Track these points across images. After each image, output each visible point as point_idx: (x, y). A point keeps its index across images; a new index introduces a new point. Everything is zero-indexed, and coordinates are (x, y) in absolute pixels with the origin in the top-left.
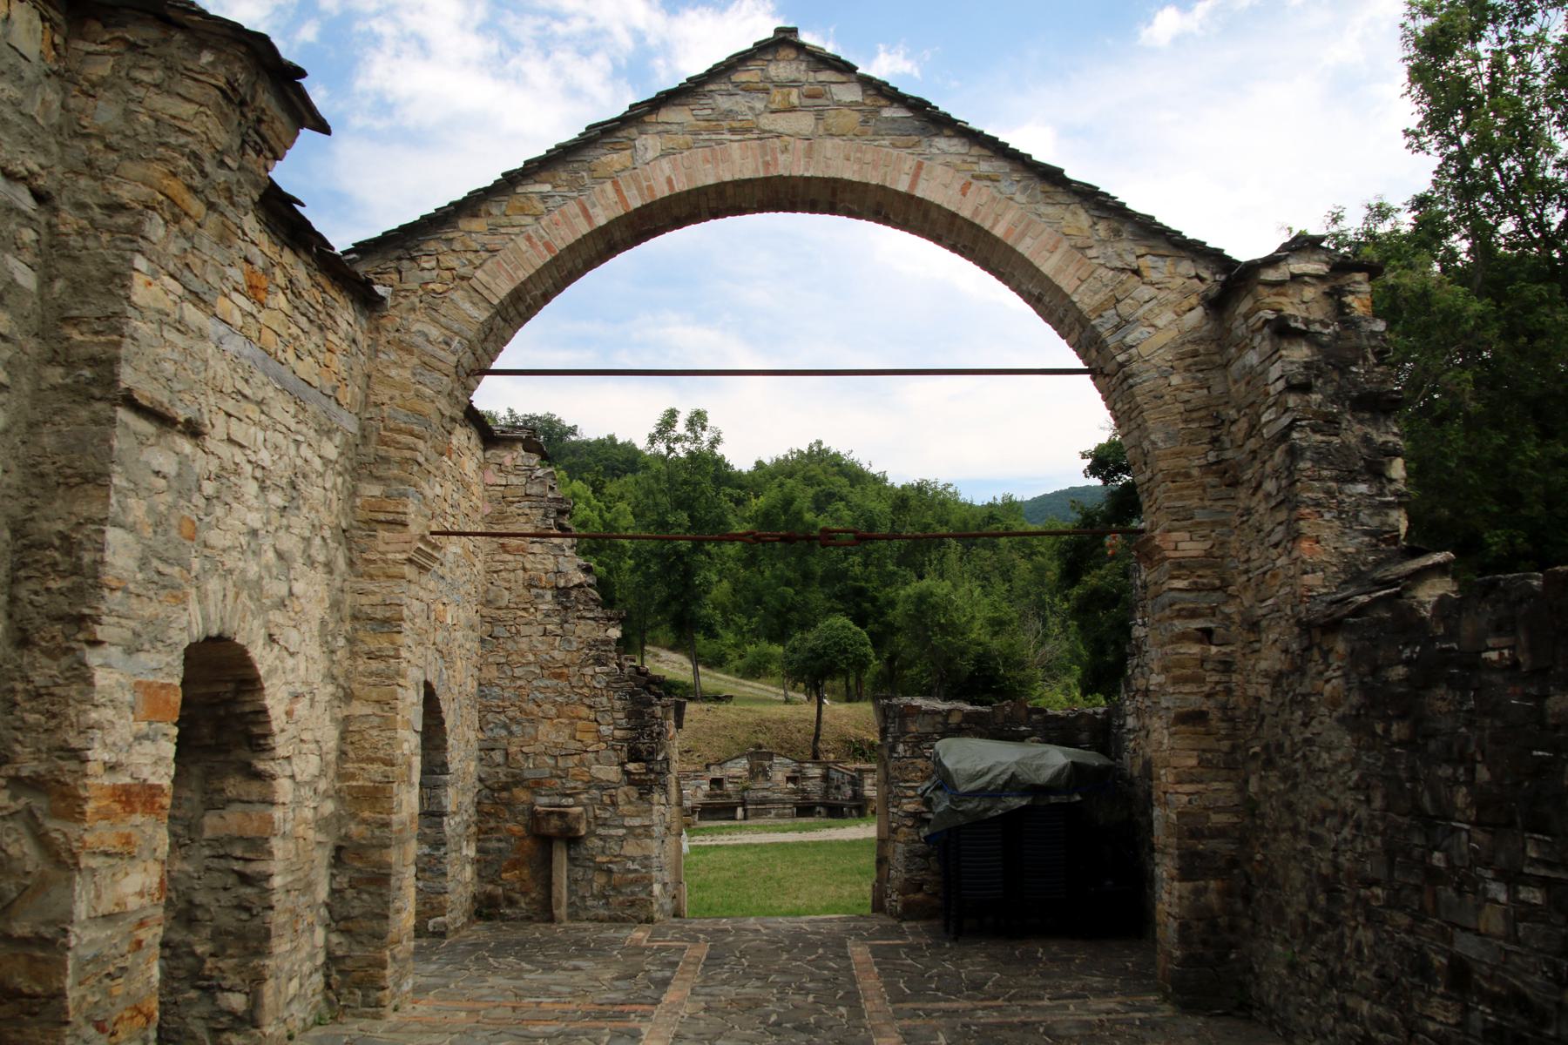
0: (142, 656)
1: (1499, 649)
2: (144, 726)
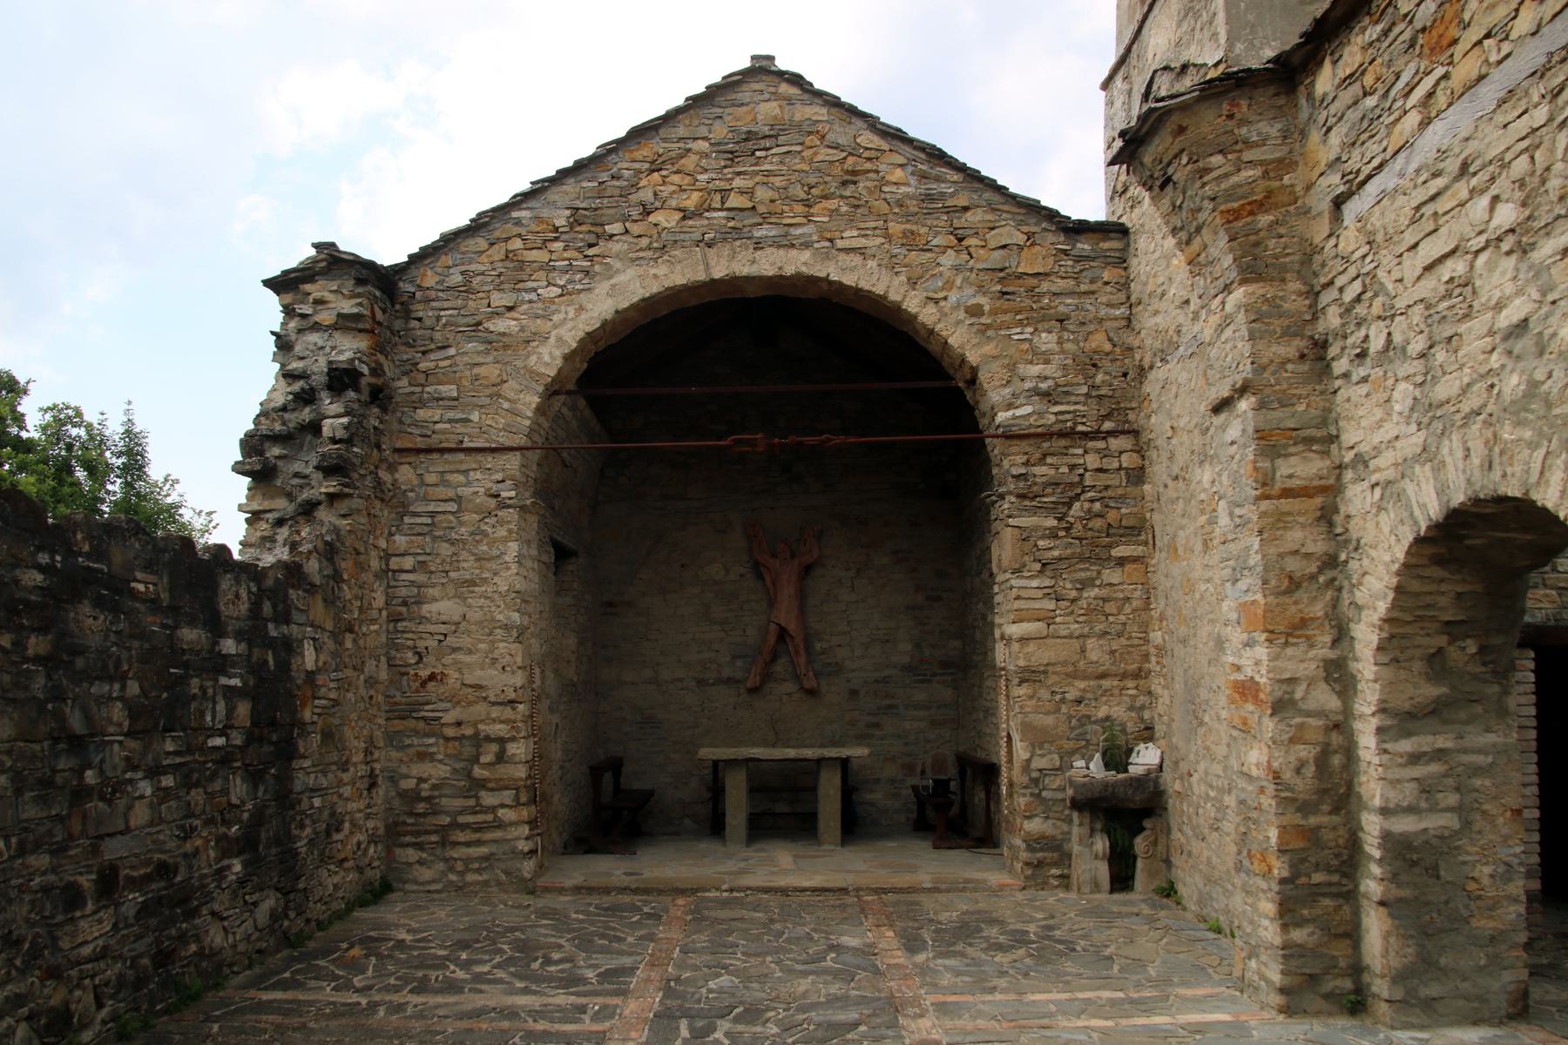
1: (146, 583)
2: (1245, 635)
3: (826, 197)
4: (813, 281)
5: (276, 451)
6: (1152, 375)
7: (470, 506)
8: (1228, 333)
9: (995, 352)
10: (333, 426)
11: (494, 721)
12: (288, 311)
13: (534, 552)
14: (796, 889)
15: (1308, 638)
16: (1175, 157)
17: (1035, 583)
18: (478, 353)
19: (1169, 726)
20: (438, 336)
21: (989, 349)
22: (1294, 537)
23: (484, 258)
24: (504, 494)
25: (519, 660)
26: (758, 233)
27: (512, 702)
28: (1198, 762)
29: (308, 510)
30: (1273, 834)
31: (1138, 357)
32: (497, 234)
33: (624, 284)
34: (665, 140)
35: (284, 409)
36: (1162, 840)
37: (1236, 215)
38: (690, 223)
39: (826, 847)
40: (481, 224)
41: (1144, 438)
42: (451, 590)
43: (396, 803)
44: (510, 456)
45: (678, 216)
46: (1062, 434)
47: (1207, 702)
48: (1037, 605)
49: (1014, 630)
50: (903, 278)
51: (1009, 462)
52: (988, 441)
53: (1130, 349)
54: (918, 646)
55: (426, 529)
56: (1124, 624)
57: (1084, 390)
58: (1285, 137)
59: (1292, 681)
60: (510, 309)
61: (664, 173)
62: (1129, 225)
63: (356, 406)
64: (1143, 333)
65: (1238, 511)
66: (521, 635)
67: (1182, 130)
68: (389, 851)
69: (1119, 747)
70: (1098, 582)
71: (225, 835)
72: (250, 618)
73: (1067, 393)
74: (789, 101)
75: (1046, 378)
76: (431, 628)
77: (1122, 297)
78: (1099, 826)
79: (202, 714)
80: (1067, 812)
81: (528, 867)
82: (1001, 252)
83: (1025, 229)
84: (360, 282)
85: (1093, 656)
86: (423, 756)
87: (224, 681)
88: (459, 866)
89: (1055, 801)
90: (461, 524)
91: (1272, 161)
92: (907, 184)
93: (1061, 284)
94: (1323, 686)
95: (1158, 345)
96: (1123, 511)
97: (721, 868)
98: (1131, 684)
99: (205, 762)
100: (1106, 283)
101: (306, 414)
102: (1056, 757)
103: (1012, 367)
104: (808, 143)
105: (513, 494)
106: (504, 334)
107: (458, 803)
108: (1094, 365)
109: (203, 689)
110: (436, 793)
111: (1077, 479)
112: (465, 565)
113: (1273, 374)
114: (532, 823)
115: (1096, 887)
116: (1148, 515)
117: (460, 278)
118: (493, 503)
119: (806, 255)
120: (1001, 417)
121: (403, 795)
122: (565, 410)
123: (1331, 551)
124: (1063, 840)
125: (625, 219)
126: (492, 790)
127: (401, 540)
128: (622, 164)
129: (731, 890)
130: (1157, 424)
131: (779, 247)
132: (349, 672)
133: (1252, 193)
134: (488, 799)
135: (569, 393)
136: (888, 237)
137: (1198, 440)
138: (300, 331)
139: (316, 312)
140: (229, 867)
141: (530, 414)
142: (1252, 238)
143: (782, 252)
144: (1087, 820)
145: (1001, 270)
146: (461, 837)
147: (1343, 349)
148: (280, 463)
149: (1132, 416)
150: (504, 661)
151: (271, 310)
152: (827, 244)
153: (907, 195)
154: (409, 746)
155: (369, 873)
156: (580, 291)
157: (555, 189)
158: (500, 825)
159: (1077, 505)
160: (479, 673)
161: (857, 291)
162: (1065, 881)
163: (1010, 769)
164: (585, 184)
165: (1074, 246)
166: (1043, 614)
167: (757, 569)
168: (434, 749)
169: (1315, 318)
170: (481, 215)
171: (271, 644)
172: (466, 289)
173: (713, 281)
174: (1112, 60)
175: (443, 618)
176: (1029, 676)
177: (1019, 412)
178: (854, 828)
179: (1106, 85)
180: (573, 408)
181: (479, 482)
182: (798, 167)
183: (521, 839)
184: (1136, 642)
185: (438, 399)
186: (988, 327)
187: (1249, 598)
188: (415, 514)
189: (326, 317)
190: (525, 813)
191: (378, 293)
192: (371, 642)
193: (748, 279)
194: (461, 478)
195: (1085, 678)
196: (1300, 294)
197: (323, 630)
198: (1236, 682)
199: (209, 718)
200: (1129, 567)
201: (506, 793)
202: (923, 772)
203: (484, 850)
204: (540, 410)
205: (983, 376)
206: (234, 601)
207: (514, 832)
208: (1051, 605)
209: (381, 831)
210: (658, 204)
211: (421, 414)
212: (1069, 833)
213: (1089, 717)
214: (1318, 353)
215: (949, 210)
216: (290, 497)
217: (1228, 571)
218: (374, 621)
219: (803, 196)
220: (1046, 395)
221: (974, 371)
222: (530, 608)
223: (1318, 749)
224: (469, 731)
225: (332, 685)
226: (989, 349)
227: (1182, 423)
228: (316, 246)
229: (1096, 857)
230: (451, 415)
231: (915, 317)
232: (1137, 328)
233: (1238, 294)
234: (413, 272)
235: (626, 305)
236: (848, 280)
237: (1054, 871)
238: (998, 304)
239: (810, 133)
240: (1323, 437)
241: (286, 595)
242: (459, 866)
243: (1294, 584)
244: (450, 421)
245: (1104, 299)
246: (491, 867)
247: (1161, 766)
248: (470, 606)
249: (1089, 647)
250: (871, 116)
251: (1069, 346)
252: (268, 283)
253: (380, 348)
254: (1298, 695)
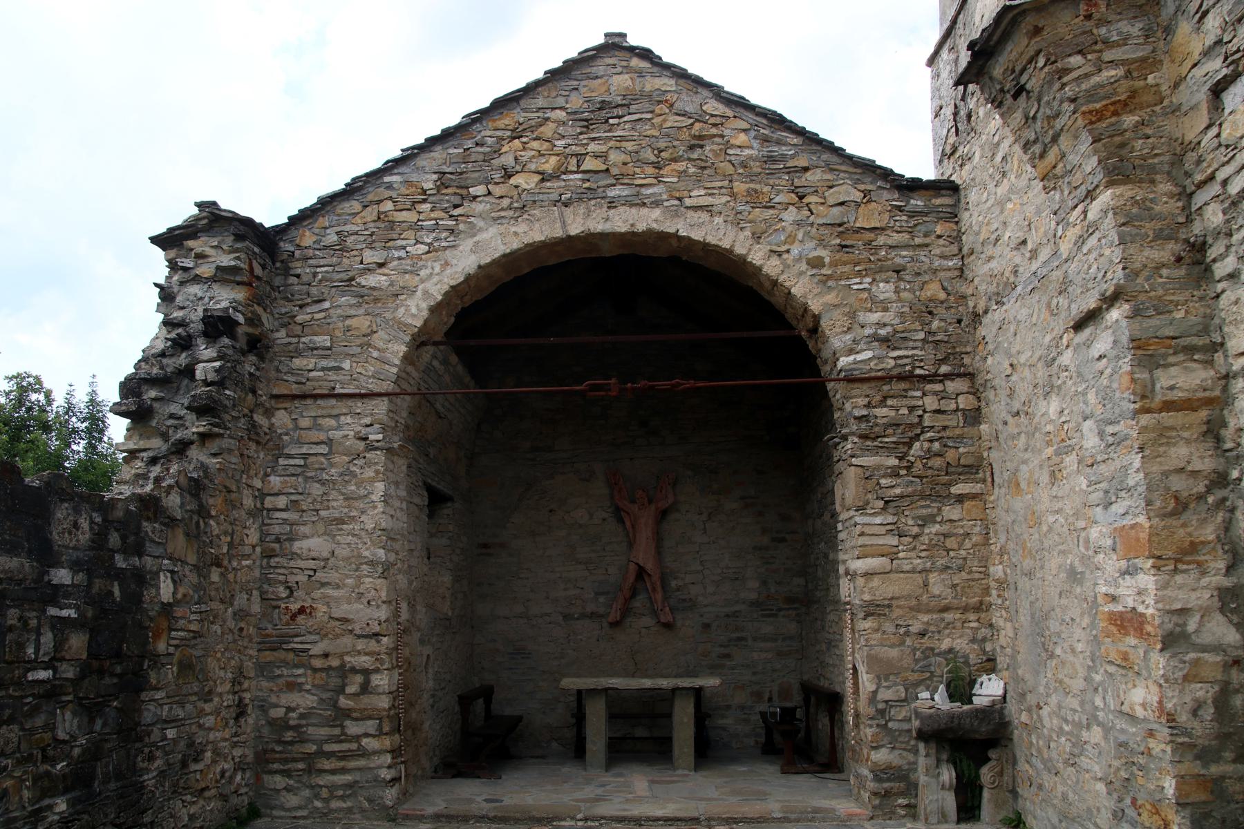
0: (1114, 507)
2: (1123, 563)
3: (675, 160)
4: (663, 237)
5: (153, 393)
6: (986, 320)
7: (340, 449)
8: (1092, 241)
9: (836, 302)
11: (359, 652)
12: (173, 265)
13: (404, 494)
14: (649, 819)
15: (1199, 564)
16: (1030, 62)
17: (878, 520)
18: (351, 306)
19: (1013, 657)
20: (314, 291)
21: (830, 298)
22: (1179, 453)
23: (358, 220)
24: (372, 437)
25: (384, 594)
26: (612, 193)
27: (376, 635)
28: (1048, 695)
29: (181, 449)
30: (1170, 786)
31: (971, 304)
32: (370, 197)
34: (525, 110)
35: (163, 354)
36: (1008, 771)
37: (1099, 115)
38: (548, 184)
39: (680, 772)
40: (353, 189)
41: (979, 380)
42: (321, 528)
43: (266, 731)
44: (378, 401)
45: (537, 178)
46: (901, 378)
47: (1059, 634)
48: (881, 541)
49: (859, 565)
50: (748, 233)
51: (851, 405)
52: (830, 386)
53: (964, 297)
54: (764, 583)
55: (299, 470)
56: (965, 559)
57: (921, 335)
58: (1147, 37)
59: (1183, 611)
60: (381, 265)
61: (524, 140)
62: (959, 182)
63: (230, 352)
64: (976, 281)
65: (1110, 429)
66: (386, 571)
67: (1037, 31)
68: (258, 778)
69: (963, 679)
70: (939, 519)
71: (48, 773)
72: (91, 548)
73: (905, 339)
74: (640, 73)
75: (885, 325)
76: (302, 564)
77: (954, 249)
78: (945, 756)
79: (21, 646)
80: (913, 742)
81: (390, 795)
82: (840, 208)
83: (862, 187)
84: (239, 237)
85: (936, 590)
86: (292, 686)
87: (53, 611)
88: (324, 793)
89: (901, 731)
90: (332, 465)
91: (1135, 61)
92: (752, 148)
93: (896, 238)
94: (1219, 617)
95: (993, 288)
96: (961, 450)
97: (579, 795)
98: (972, 617)
99: (23, 697)
100: (939, 237)
101: (183, 359)
102: (902, 689)
103: (852, 315)
104: (657, 111)
105: (380, 437)
106: (374, 289)
107: (324, 732)
108: (930, 313)
109: (23, 620)
110: (304, 722)
111: (917, 420)
112: (335, 504)
113: (1147, 279)
114: (395, 752)
115: (944, 818)
116: (985, 454)
117: (335, 238)
118: (361, 445)
119: (656, 213)
120: (844, 361)
121: (272, 723)
122: (435, 363)
123: (1221, 469)
124: (909, 770)
125: (488, 181)
126: (357, 719)
127: (275, 480)
128: (486, 132)
129: (586, 819)
130: (995, 365)
131: (632, 205)
132: (215, 605)
133: (1115, 93)
134: (353, 728)
135: (436, 344)
136: (733, 195)
137: (1042, 373)
138: (182, 283)
139: (197, 266)
140: (50, 807)
141: (397, 362)
142: (1117, 139)
143: (634, 210)
144: (933, 751)
145: (840, 225)
146: (327, 764)
147: (1228, 247)
148: (156, 405)
149: (967, 360)
150: (369, 596)
151: (157, 265)
152: (677, 202)
153: (750, 157)
154: (279, 676)
155: (235, 800)
156: (446, 248)
157: (423, 156)
158: (364, 753)
159: (917, 445)
160: (345, 606)
161: (705, 246)
162: (912, 811)
163: (856, 700)
164: (451, 151)
165: (908, 202)
166: (886, 550)
167: (618, 514)
168: (302, 680)
169: (1189, 220)
170: (355, 180)
171: (119, 575)
172: (341, 248)
173: (569, 237)
174: (936, 36)
175: (313, 554)
176: (874, 610)
177: (860, 357)
178: (708, 752)
179: (932, 61)
180: (445, 362)
181: (349, 426)
182: (649, 133)
183: (383, 767)
184: (977, 576)
185: (313, 349)
186: (829, 277)
187: (1128, 521)
188: (290, 456)
189: (206, 270)
190: (387, 743)
191: (256, 250)
192: (242, 577)
193: (603, 236)
194: (333, 422)
195: (928, 611)
196: (1171, 196)
197: (184, 563)
198: (1111, 613)
199: (30, 650)
200: (967, 504)
201: (371, 722)
202: (770, 699)
203: (348, 778)
204: (406, 358)
205: (825, 323)
206: (72, 529)
207: (376, 761)
208: (894, 541)
209: (250, 758)
210: (518, 168)
211: (297, 363)
212: (915, 763)
213: (932, 649)
214: (1196, 259)
215: (791, 171)
216: (165, 436)
217: (1100, 494)
218: (248, 557)
219: (653, 159)
220: (885, 341)
221: (817, 318)
222: (397, 546)
223: (1217, 688)
224: (335, 663)
225: (193, 617)
226: (830, 298)
227: (1023, 359)
228: (200, 205)
229: (943, 787)
230: (324, 363)
231: (760, 269)
232: (970, 277)
233: (1106, 197)
234: (293, 233)
235: (488, 260)
236: (697, 235)
237: (900, 801)
238: (838, 256)
239: (659, 102)
240: (1206, 345)
241: (139, 527)
242: (324, 793)
243: (1181, 506)
244: (323, 369)
245: (937, 251)
246: (354, 795)
247: (1004, 697)
248: (338, 543)
249: (931, 581)
250: (716, 86)
251: (905, 295)
252: (155, 240)
253: (257, 299)
254: (1192, 626)
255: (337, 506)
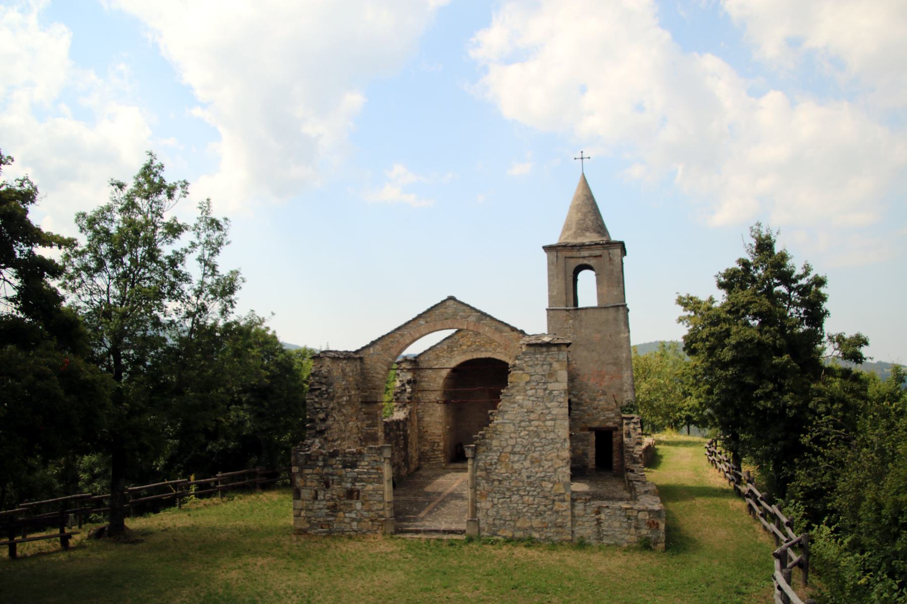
10: (409, 390)
33: (457, 360)
40: (430, 349)
86: (425, 445)
183: (442, 460)
255: (431, 412)
